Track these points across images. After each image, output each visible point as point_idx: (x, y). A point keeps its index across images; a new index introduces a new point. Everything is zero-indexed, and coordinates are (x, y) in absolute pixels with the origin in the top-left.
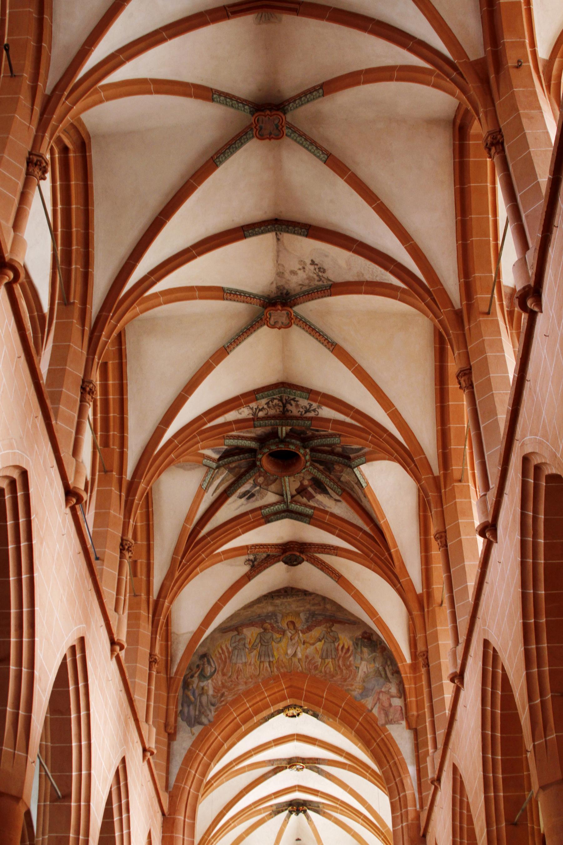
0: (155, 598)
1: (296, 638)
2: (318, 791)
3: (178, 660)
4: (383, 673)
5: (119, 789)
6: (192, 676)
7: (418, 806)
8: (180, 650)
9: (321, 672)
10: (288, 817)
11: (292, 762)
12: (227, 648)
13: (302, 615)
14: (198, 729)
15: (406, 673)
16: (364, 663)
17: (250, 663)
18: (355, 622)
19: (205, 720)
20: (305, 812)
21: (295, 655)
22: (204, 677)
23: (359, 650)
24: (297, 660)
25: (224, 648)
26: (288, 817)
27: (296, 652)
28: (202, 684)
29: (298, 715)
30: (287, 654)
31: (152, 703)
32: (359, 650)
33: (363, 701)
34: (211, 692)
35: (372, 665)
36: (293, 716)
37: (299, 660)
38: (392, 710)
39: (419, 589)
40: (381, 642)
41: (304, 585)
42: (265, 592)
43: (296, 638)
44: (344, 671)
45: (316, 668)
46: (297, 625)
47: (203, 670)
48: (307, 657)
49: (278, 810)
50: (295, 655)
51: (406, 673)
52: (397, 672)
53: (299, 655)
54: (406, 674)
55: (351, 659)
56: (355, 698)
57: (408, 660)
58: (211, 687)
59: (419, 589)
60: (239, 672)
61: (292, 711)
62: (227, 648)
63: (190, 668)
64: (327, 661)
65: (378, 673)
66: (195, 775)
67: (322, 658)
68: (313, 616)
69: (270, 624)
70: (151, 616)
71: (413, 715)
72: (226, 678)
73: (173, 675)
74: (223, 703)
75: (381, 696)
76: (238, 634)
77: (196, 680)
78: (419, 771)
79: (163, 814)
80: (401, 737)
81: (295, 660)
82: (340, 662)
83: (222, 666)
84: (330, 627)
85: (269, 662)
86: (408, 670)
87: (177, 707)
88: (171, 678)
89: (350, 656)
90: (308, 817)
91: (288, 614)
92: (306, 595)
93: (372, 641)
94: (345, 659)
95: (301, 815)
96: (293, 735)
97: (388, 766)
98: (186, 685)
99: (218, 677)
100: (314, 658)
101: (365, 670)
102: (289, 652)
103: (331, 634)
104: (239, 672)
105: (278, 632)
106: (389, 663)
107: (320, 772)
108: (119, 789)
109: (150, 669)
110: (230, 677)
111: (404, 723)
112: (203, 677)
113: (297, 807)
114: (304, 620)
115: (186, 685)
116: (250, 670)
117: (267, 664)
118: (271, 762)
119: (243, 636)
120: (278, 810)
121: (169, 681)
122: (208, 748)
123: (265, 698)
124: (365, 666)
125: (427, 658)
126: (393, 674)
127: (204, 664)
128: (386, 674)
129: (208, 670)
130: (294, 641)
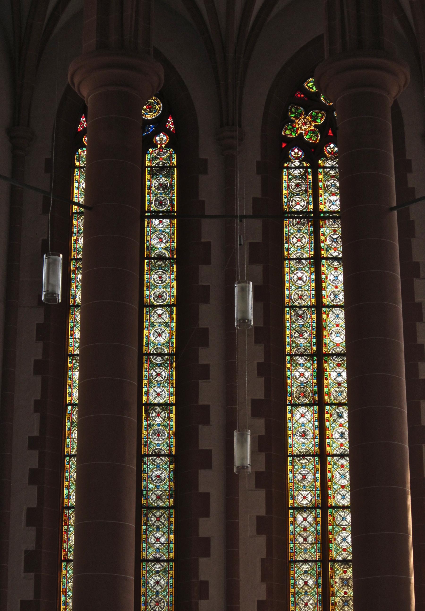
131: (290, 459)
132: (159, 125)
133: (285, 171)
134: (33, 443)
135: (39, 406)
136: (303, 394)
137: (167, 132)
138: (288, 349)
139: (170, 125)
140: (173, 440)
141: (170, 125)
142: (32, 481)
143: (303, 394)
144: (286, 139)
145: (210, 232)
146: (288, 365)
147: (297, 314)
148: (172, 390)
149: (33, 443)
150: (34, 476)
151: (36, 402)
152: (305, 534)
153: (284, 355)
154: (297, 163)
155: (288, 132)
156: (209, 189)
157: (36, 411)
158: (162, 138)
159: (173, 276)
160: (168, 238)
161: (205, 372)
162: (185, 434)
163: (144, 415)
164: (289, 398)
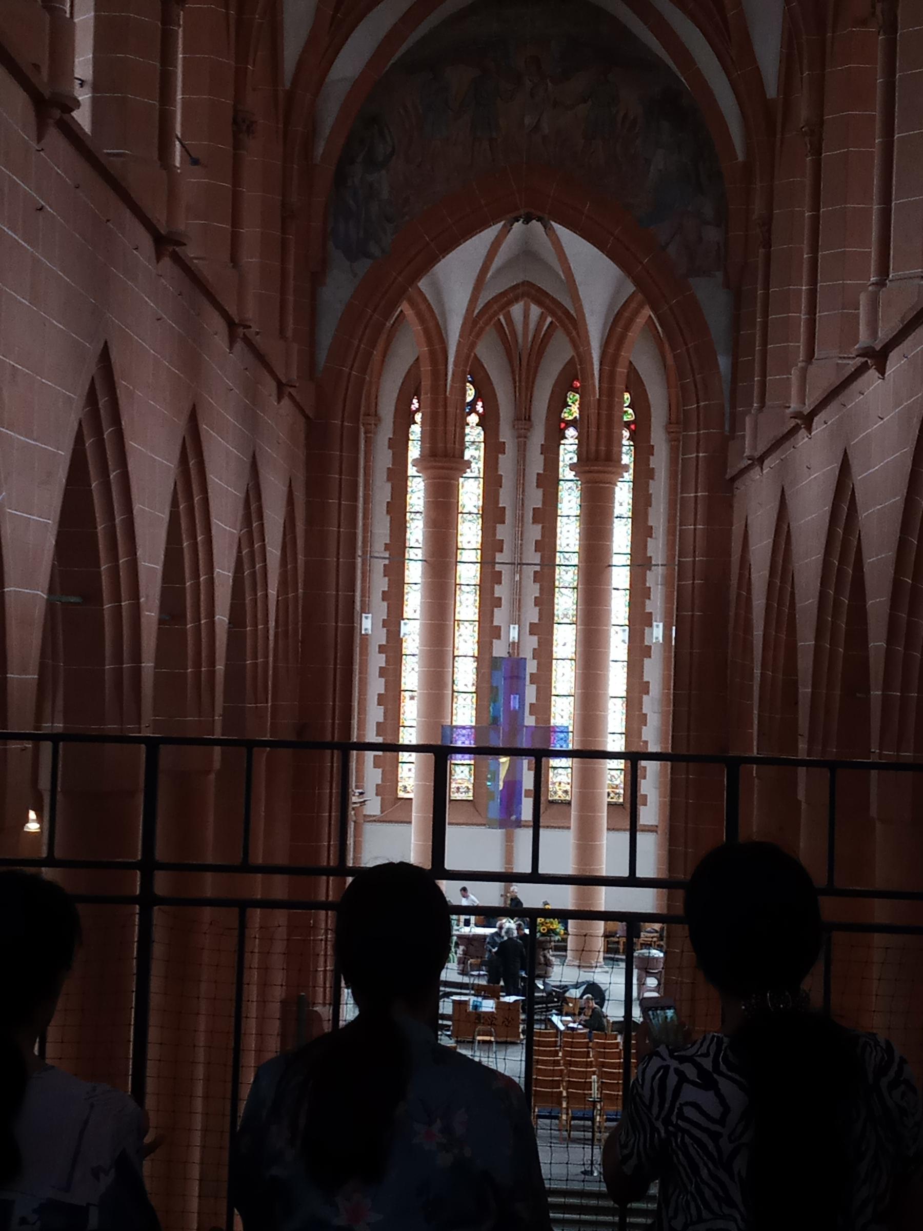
0: (288, 85)
5: (250, 533)
7: (727, 428)
14: (364, 266)
19: (374, 249)
21: (537, 128)
27: (539, 120)
31: (291, 298)
34: (385, 195)
39: (772, 90)
50: (537, 128)
57: (741, 157)
59: (772, 90)
66: (359, 346)
70: (281, 126)
74: (407, 218)
78: (735, 366)
79: (307, 417)
80: (712, 299)
93: (680, 108)
97: (684, 348)
98: (340, 178)
102: (527, 120)
108: (250, 533)
109: (284, 230)
111: (719, 275)
125: (769, 231)
131: (554, 662)
132: (473, 404)
133: (562, 447)
134: (382, 649)
136: (565, 616)
137: (477, 413)
138: (557, 583)
139: (479, 407)
140: (476, 646)
141: (479, 407)
142: (381, 676)
143: (565, 616)
144: (563, 420)
145: (505, 499)
146: (557, 595)
147: (564, 558)
148: (477, 611)
149: (382, 649)
150: (382, 672)
151: (384, 620)
152: (562, 713)
153: (554, 587)
154: (571, 441)
155: (566, 415)
156: (506, 463)
157: (384, 627)
158: (473, 419)
159: (480, 527)
160: (476, 498)
161: (498, 602)
163: (456, 628)
164: (556, 618)
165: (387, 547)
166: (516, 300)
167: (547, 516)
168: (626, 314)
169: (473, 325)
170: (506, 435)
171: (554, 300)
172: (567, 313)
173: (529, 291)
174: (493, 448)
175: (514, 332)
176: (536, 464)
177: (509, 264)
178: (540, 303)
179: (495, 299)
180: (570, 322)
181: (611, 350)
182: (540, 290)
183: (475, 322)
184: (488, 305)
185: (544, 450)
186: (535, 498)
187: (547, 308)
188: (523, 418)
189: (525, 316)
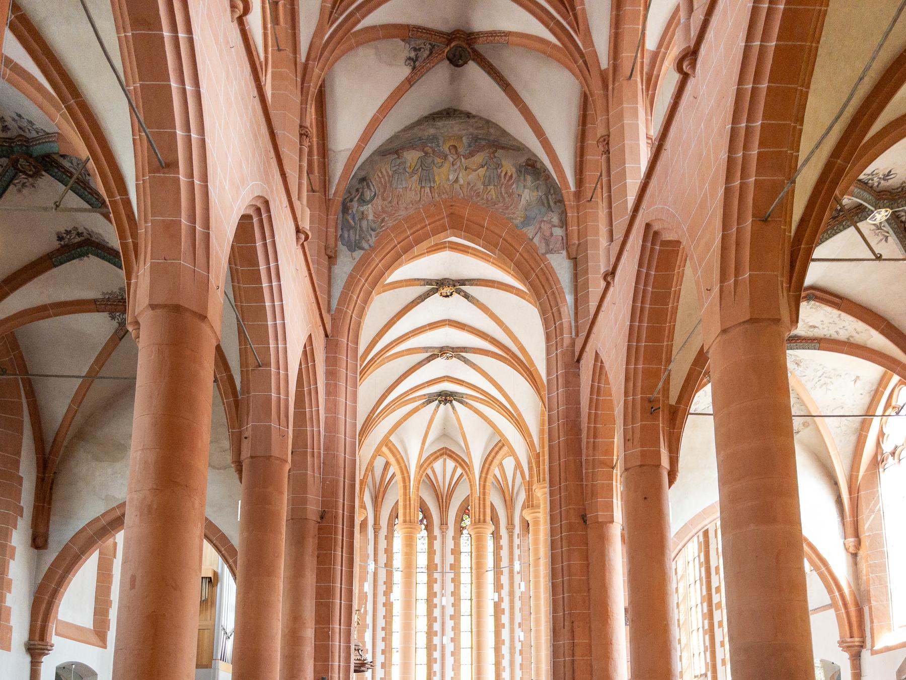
1: (458, 164)
2: (463, 381)
3: (336, 181)
4: (545, 202)
6: (351, 201)
8: (338, 169)
9: (483, 199)
10: (438, 406)
11: (442, 351)
12: (387, 172)
13: (464, 140)
15: (569, 201)
16: (526, 191)
17: (411, 190)
18: (518, 148)
20: (451, 401)
21: (456, 181)
22: (364, 201)
23: (522, 178)
24: (458, 187)
25: (384, 173)
26: (438, 406)
28: (362, 209)
29: (451, 294)
30: (448, 179)
32: (522, 178)
33: (525, 230)
35: (535, 194)
36: (447, 296)
37: (461, 186)
38: (553, 239)
40: (545, 170)
41: (469, 104)
42: (426, 113)
43: (458, 164)
44: (507, 200)
45: (478, 195)
46: (459, 150)
47: (362, 194)
48: (469, 183)
49: (430, 399)
50: (456, 181)
51: (569, 201)
52: (560, 201)
53: (461, 182)
54: (570, 201)
55: (514, 186)
56: (517, 226)
58: (370, 211)
60: (399, 197)
61: (447, 290)
62: (387, 172)
63: (349, 192)
64: (489, 188)
65: (540, 202)
67: (484, 184)
68: (476, 141)
69: (431, 147)
71: (574, 244)
72: (385, 202)
73: (331, 197)
75: (542, 226)
76: (398, 158)
77: (355, 204)
81: (457, 186)
82: (503, 190)
83: (382, 190)
84: (493, 153)
85: (430, 187)
86: (572, 198)
87: (336, 232)
88: (329, 200)
89: (512, 184)
90: (453, 408)
91: (450, 137)
92: (468, 117)
94: (508, 187)
95: (448, 404)
96: (444, 321)
98: (345, 209)
99: (378, 202)
100: (475, 185)
101: (528, 198)
103: (495, 160)
104: (399, 197)
105: (439, 156)
106: (552, 192)
107: (466, 361)
110: (390, 202)
112: (363, 201)
113: (446, 397)
114: (466, 144)
115: (345, 209)
116: (411, 196)
117: (428, 190)
118: (426, 349)
119: (403, 160)
120: (430, 399)
121: (327, 203)
122: (367, 279)
123: (426, 226)
124: (527, 194)
126: (555, 203)
127: (363, 188)
128: (549, 203)
129: (368, 195)
130: (455, 167)
132: (421, 521)
135: (384, 617)
139: (425, 522)
141: (425, 522)
145: (437, 559)
156: (437, 545)
158: (423, 527)
162: (430, 627)
165: (385, 583)
166: (441, 455)
167: (456, 567)
168: (490, 458)
169: (421, 467)
170: (437, 532)
171: (457, 455)
172: (463, 460)
173: (445, 453)
174: (431, 538)
175: (439, 486)
176: (450, 544)
177: (438, 439)
178: (451, 457)
179: (432, 455)
180: (463, 463)
181: (484, 475)
182: (450, 451)
183: (422, 466)
184: (428, 458)
185: (454, 538)
186: (450, 559)
187: (455, 460)
188: (444, 523)
189: (444, 469)
